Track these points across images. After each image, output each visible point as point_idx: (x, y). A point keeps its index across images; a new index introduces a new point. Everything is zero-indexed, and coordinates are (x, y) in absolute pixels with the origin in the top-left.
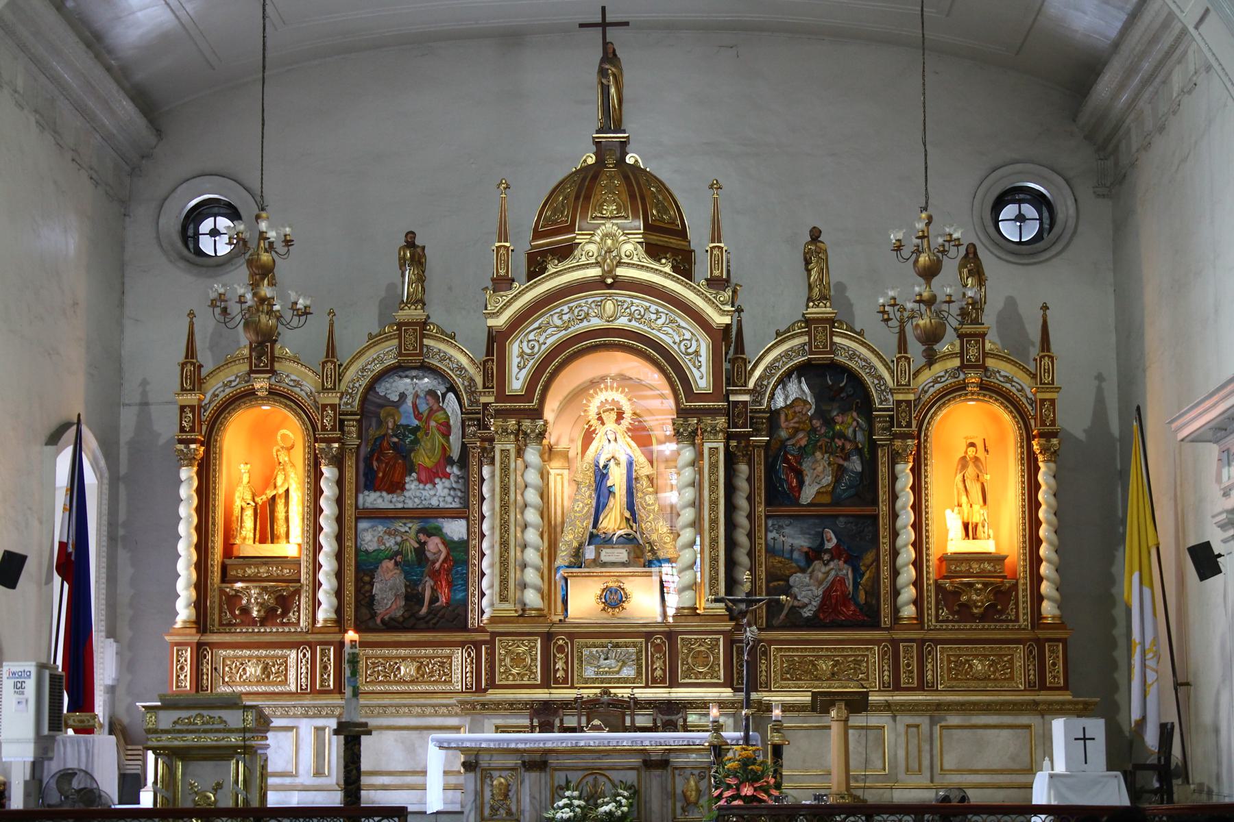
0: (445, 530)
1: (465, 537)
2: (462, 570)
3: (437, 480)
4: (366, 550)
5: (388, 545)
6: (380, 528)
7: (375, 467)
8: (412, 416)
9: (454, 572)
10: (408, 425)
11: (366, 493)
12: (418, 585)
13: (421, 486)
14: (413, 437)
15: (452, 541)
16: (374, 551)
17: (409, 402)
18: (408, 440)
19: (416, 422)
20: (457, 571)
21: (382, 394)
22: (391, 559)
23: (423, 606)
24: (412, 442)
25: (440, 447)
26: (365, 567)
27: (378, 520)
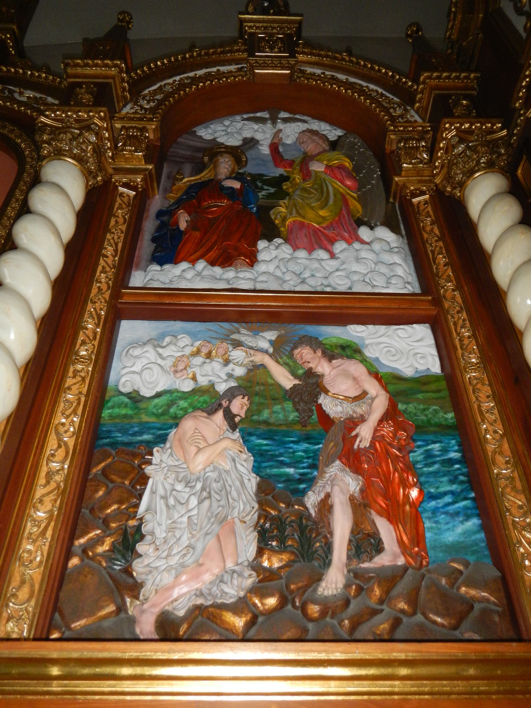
0: (369, 353)
1: (436, 368)
2: (445, 450)
3: (339, 247)
4: (137, 392)
5: (203, 381)
6: (184, 340)
7: (183, 225)
8: (271, 164)
9: (417, 456)
10: (262, 175)
11: (155, 267)
12: (304, 492)
13: (302, 254)
14: (272, 190)
15: (398, 378)
16: (158, 395)
17: (265, 150)
18: (264, 193)
19: (280, 171)
20: (429, 455)
21: (208, 137)
22: (211, 412)
23: (327, 563)
24: (270, 196)
25: (339, 196)
26: (120, 437)
27: (178, 325)
